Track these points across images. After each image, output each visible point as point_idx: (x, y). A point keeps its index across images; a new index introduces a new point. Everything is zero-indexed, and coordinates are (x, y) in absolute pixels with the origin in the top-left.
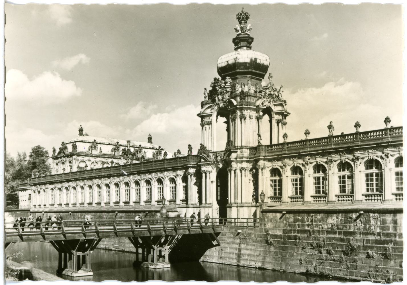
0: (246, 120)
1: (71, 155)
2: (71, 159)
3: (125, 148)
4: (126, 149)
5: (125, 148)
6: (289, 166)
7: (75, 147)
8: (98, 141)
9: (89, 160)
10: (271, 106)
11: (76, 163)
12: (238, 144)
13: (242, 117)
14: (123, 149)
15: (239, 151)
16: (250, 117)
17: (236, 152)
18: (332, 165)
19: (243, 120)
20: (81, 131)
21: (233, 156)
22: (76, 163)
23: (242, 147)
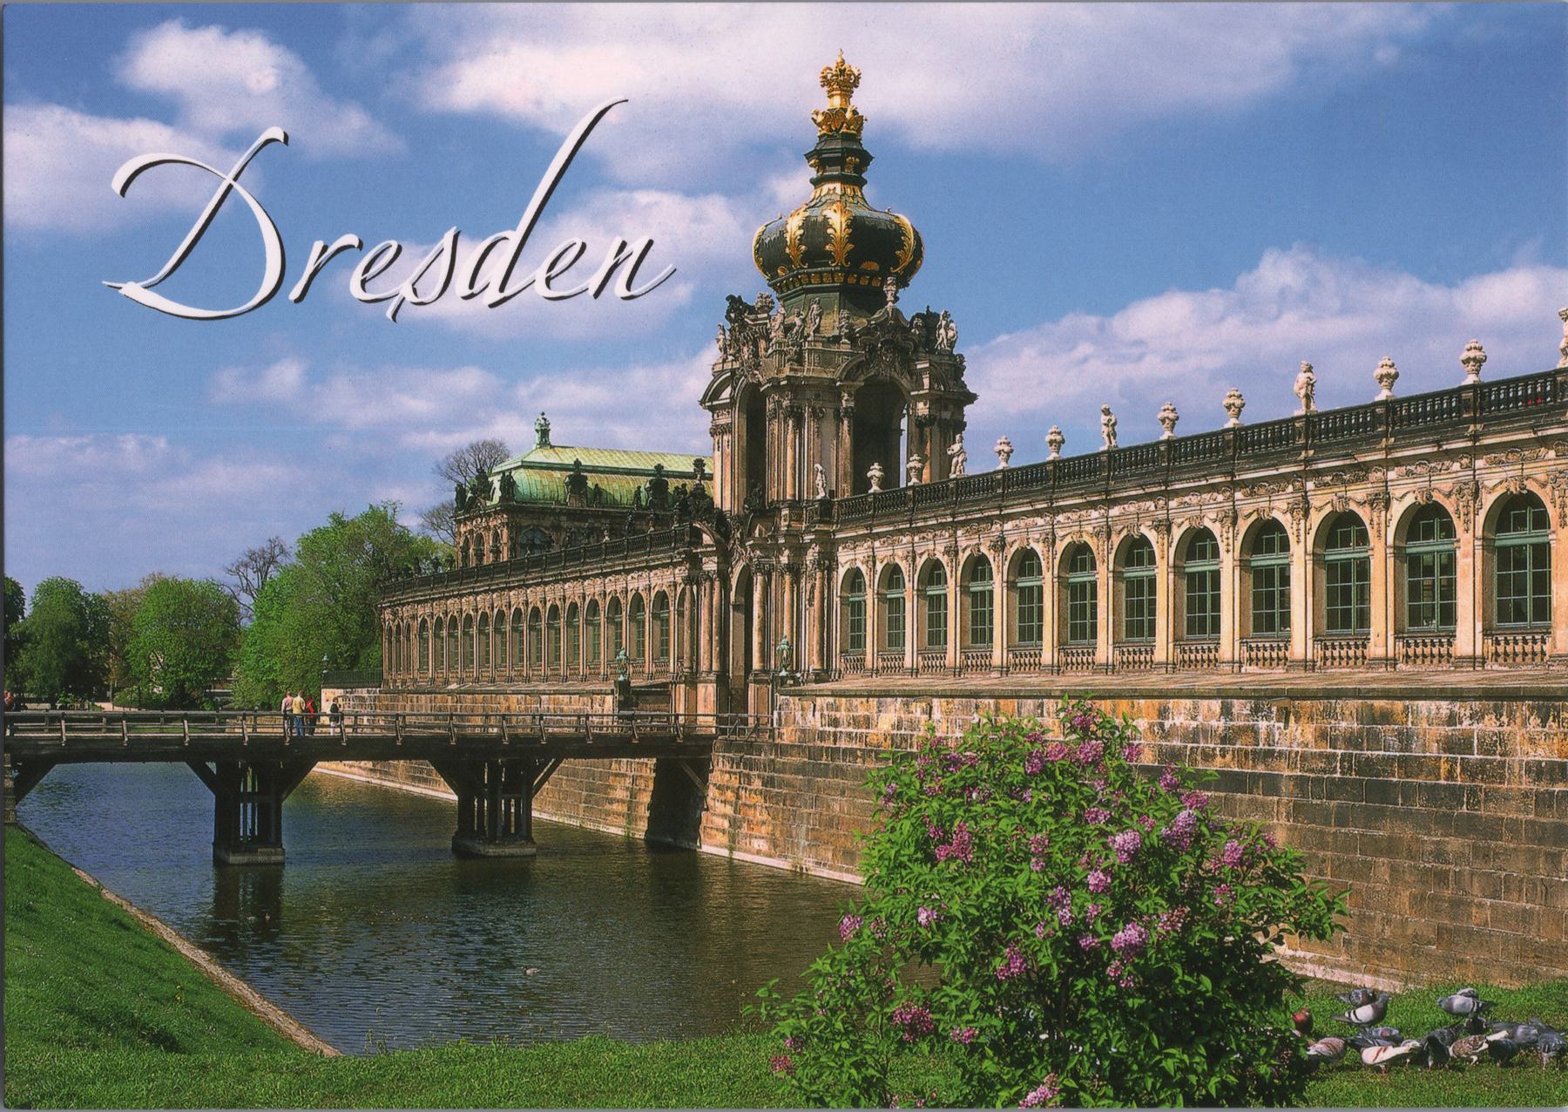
3: (684, 485)
4: (689, 489)
5: (684, 485)
14: (677, 488)
20: (544, 432)
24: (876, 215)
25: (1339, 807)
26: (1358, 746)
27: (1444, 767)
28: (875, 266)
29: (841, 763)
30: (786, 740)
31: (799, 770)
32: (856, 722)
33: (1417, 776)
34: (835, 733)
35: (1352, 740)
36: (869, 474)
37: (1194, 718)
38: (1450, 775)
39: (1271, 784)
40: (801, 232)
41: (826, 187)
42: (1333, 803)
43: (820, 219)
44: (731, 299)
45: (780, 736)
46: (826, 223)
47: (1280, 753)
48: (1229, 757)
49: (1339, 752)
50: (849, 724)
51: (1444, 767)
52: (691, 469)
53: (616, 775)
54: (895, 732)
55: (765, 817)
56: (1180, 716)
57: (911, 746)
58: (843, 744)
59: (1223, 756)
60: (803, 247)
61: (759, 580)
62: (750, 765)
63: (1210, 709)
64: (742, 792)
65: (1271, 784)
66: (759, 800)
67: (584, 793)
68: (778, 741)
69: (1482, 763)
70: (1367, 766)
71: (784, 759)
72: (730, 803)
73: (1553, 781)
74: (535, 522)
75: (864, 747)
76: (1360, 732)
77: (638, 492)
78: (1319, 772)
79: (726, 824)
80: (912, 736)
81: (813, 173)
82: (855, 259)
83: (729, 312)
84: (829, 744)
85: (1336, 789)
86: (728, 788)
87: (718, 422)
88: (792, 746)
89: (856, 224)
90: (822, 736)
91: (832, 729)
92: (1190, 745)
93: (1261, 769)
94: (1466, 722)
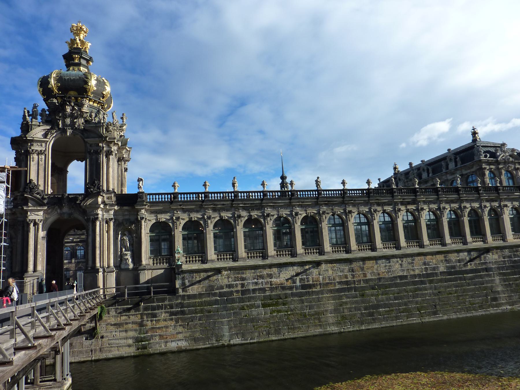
6: (183, 219)
35: (510, 257)
37: (457, 257)
48: (473, 265)
55: (180, 329)
56: (453, 257)
57: (308, 281)
58: (251, 287)
66: (173, 323)
75: (269, 286)
78: (501, 265)
79: (130, 341)
80: (307, 278)
84: (239, 288)
86: (127, 323)
90: (229, 286)
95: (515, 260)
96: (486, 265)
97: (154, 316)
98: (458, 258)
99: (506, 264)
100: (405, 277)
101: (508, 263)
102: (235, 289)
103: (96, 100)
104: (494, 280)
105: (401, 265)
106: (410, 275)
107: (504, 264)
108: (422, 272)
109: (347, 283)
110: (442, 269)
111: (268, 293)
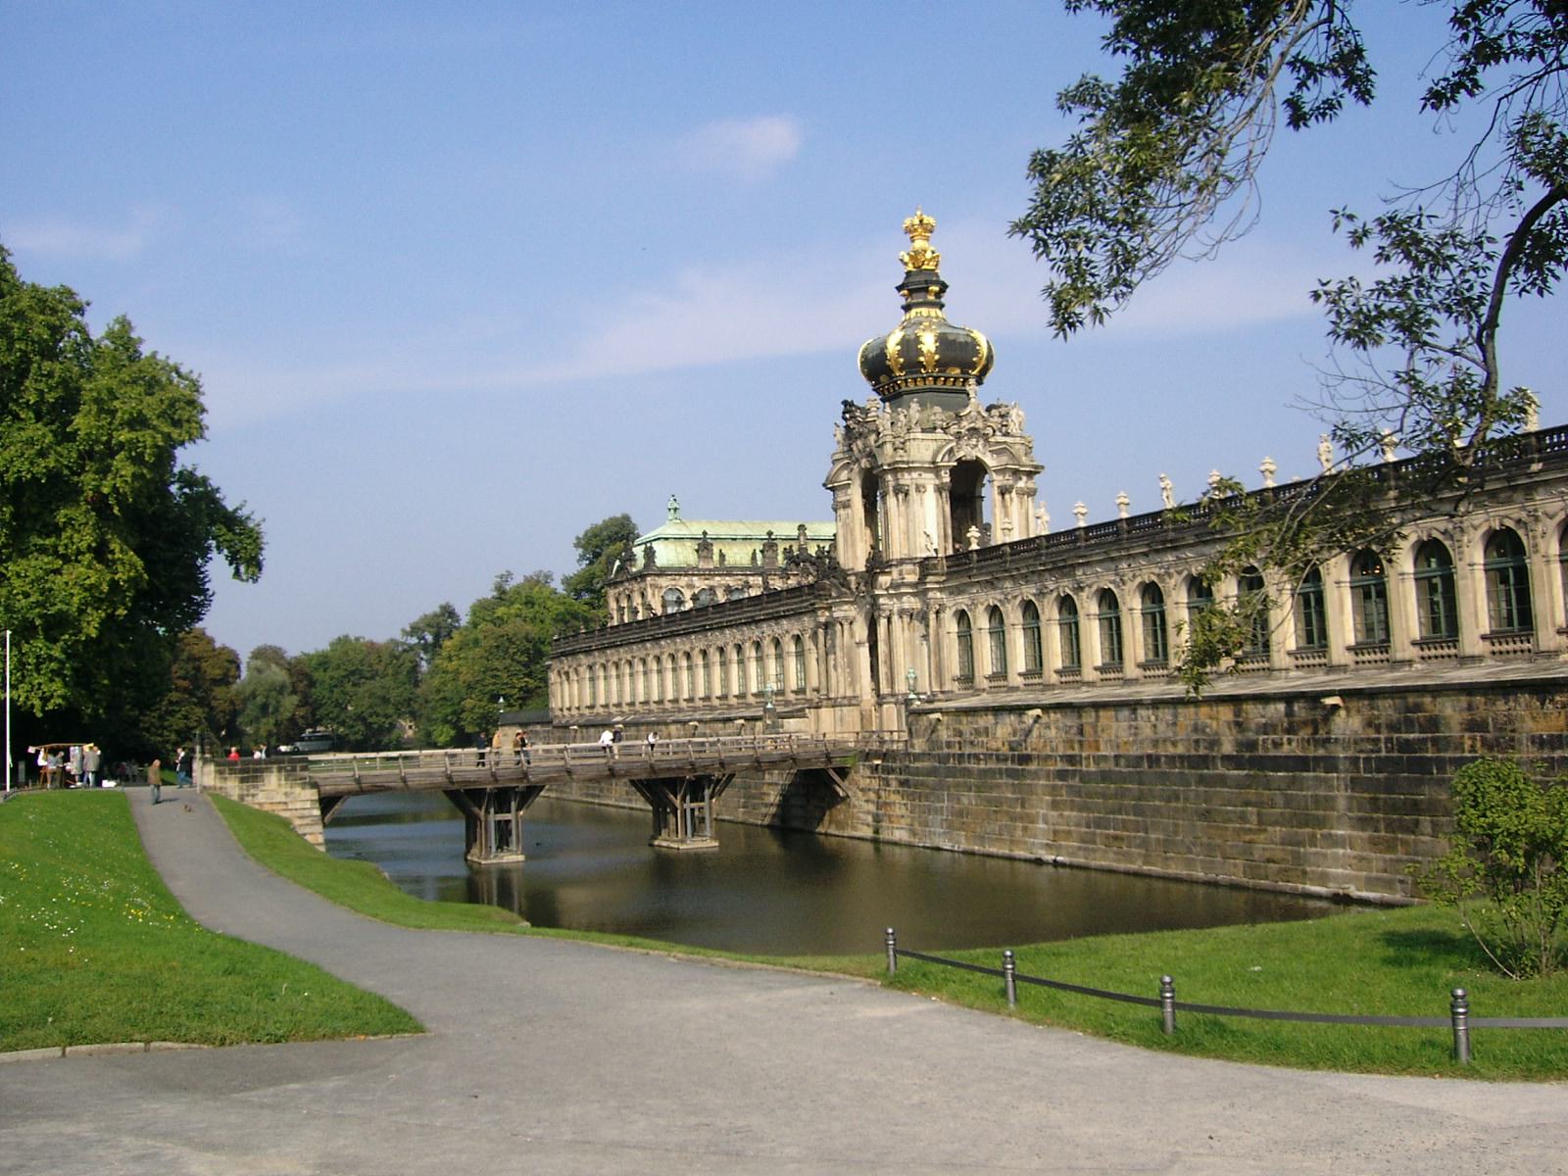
0: (910, 497)
1: (641, 576)
2: (642, 585)
7: (650, 554)
8: (712, 532)
9: (690, 586)
10: (980, 455)
11: (654, 595)
12: (897, 551)
13: (901, 490)
15: (895, 571)
16: (918, 489)
17: (890, 573)
18: (1046, 600)
19: (901, 496)
21: (884, 580)
22: (654, 595)
23: (902, 562)
24: (955, 331)
25: (1386, 778)
26: (1399, 731)
27: (1468, 743)
28: (958, 371)
29: (967, 765)
30: (917, 750)
31: (932, 772)
32: (977, 732)
33: (1446, 750)
34: (959, 743)
35: (1393, 727)
36: (969, 535)
37: (1263, 717)
38: (1473, 749)
39: (1330, 763)
40: (899, 348)
41: (913, 312)
42: (1381, 776)
43: (913, 337)
44: (845, 403)
45: (913, 746)
46: (917, 340)
47: (1336, 740)
48: (1294, 744)
49: (1382, 736)
50: (971, 734)
51: (1468, 743)
52: (795, 533)
53: (769, 784)
54: (1013, 739)
55: (903, 811)
56: (1255, 713)
58: (967, 750)
59: (1289, 743)
60: (902, 360)
61: (883, 622)
62: (890, 771)
63: (1276, 709)
64: (882, 793)
65: (1330, 763)
67: (742, 800)
68: (910, 750)
69: (1497, 739)
70: (1405, 746)
71: (917, 764)
72: (873, 802)
73: (1553, 749)
74: (673, 583)
75: (985, 751)
76: (1399, 721)
77: (754, 553)
79: (870, 819)
81: (903, 302)
82: (942, 365)
83: (844, 413)
84: (956, 750)
85: (1382, 765)
87: (839, 500)
88: (923, 754)
89: (942, 340)
90: (949, 745)
91: (958, 739)
92: (1261, 738)
93: (1321, 752)
94: (1482, 707)
95: (1407, 740)
96: (1326, 749)
97: (888, 785)
98: (1263, 720)
99: (1379, 751)
100: (1158, 758)
101: (1386, 747)
102: (951, 751)
103: (915, 376)
104: (1333, 798)
105: (1155, 726)
106: (1166, 756)
107: (1372, 751)
108: (1189, 751)
109: (1071, 759)
110: (1228, 748)
111: (982, 766)
